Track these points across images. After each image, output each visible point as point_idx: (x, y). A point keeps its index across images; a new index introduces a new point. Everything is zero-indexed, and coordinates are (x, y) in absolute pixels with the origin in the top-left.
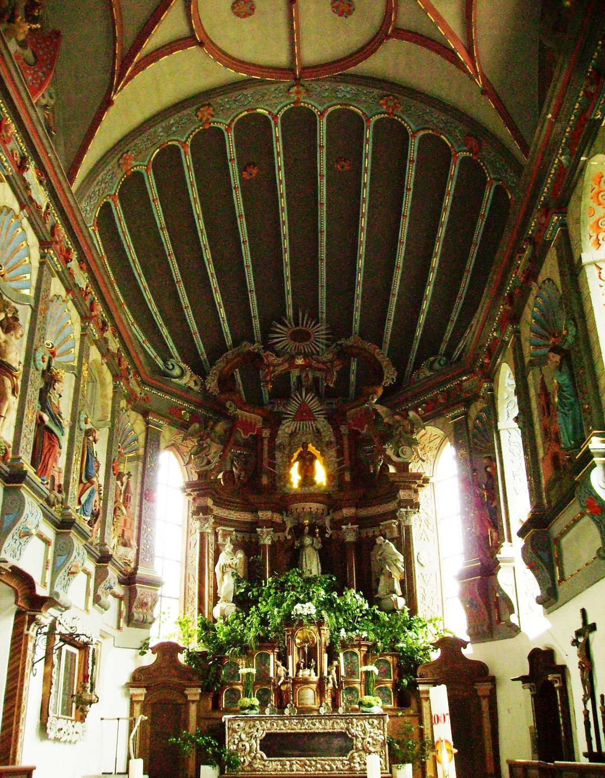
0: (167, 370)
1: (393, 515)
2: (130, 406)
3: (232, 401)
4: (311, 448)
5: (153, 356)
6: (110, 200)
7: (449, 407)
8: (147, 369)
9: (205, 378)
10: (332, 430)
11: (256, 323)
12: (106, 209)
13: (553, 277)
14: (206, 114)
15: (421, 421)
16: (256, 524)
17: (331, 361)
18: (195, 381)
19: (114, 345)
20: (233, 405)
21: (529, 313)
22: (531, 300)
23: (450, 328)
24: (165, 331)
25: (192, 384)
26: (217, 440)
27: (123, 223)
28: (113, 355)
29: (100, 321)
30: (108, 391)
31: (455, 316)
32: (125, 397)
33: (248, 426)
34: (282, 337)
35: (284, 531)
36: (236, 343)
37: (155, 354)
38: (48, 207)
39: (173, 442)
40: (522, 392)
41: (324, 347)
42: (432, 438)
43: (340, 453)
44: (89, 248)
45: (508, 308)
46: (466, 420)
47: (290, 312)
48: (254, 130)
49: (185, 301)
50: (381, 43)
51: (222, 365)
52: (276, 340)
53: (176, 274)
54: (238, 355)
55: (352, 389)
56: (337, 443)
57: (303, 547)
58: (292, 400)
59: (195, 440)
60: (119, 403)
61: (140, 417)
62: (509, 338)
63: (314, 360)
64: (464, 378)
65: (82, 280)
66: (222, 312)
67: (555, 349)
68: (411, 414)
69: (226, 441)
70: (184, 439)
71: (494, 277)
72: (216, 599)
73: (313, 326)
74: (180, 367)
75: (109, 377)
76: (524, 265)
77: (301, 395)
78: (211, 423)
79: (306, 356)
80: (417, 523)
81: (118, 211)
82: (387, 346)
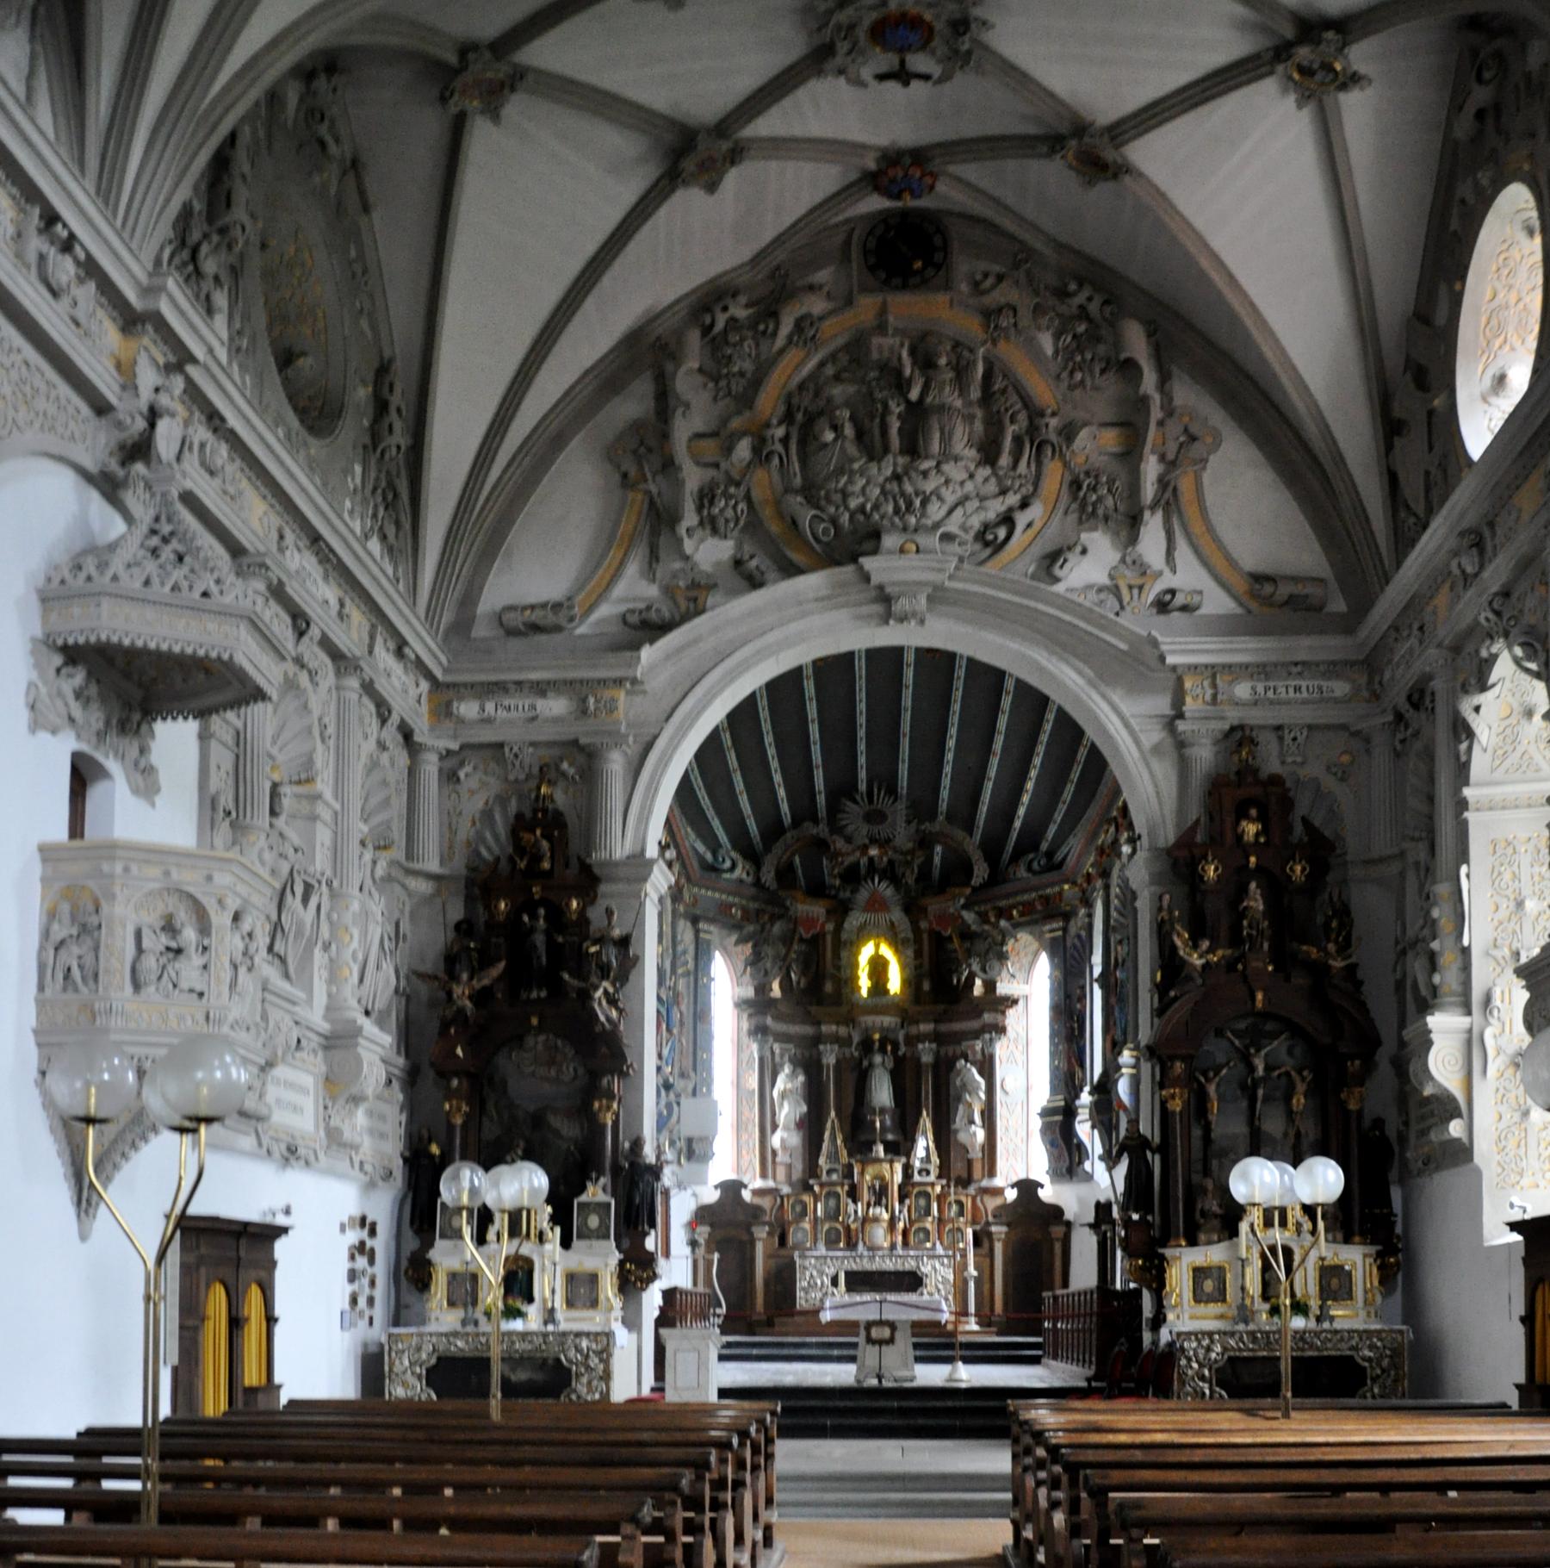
1: (976, 1035)
7: (1049, 917)
8: (696, 864)
11: (821, 800)
16: (817, 1040)
17: (912, 852)
23: (1052, 830)
31: (1058, 817)
33: (810, 922)
34: (853, 814)
35: (850, 1045)
36: (797, 822)
43: (918, 954)
46: (1064, 937)
47: (863, 787)
57: (871, 1065)
72: (775, 1127)
80: (1002, 1050)
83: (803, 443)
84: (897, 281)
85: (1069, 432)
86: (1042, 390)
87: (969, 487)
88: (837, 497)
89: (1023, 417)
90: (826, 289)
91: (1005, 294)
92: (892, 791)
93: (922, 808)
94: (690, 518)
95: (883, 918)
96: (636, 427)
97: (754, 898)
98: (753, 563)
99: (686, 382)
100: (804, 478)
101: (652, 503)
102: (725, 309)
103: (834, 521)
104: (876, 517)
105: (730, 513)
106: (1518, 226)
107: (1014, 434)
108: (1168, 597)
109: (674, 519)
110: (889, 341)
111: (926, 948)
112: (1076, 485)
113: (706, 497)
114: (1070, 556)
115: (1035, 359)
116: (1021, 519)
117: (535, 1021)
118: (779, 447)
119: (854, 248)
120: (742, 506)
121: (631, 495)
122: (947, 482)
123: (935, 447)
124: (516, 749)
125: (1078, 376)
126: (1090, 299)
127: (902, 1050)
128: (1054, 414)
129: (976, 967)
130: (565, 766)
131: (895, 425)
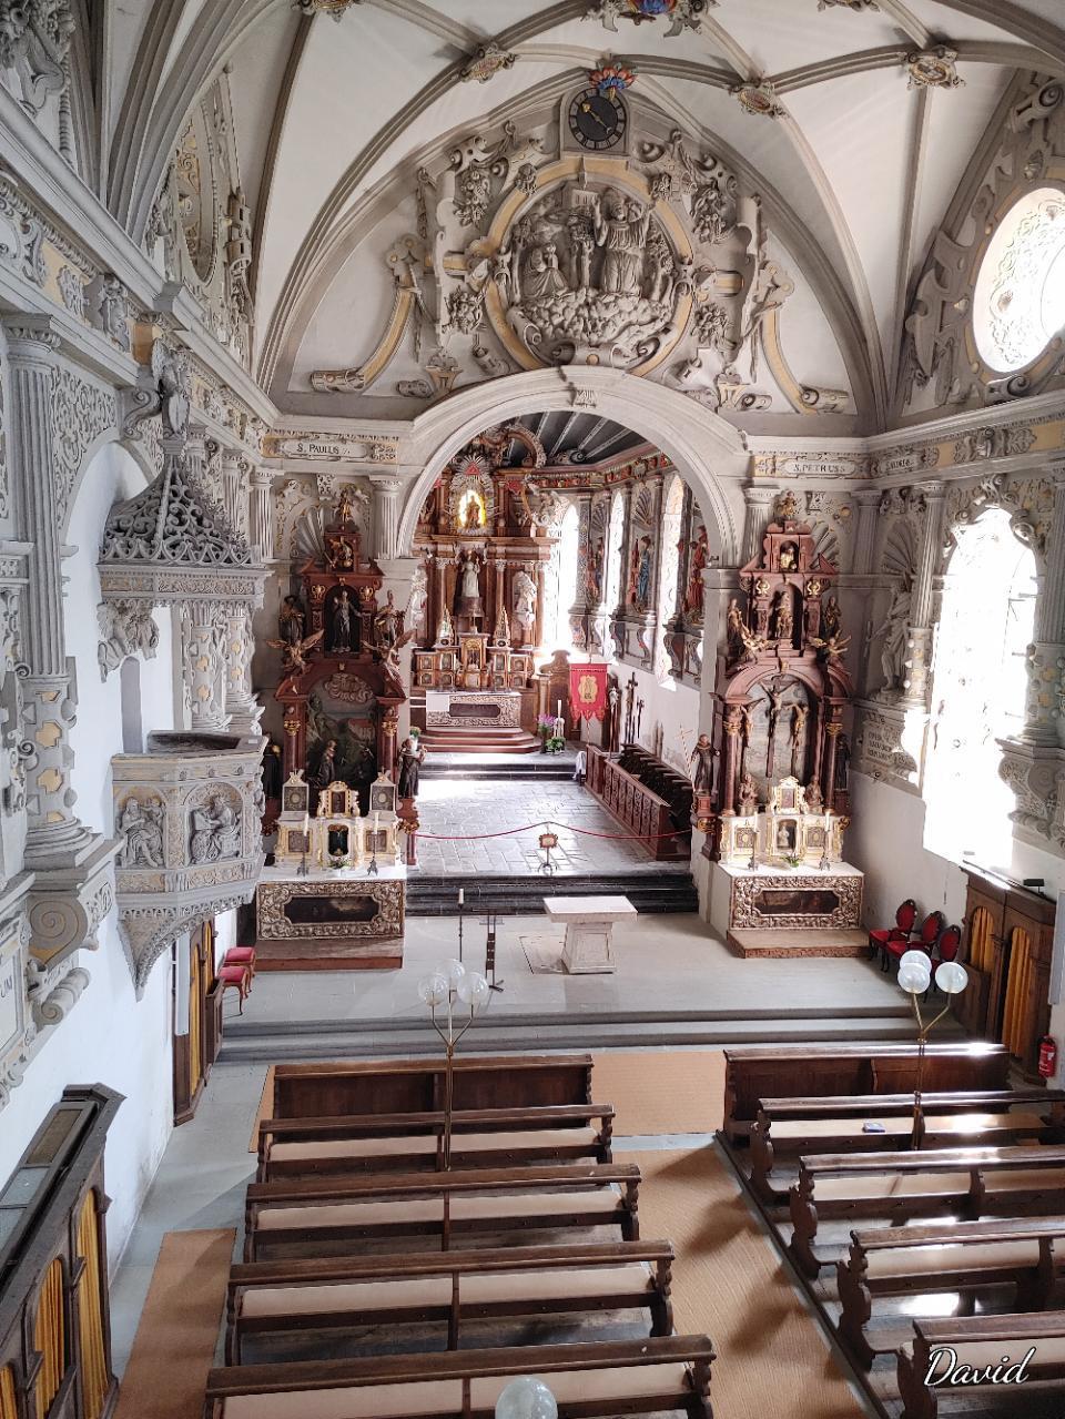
7: (580, 491)
43: (497, 503)
83: (522, 266)
84: (590, 144)
85: (700, 275)
86: (684, 240)
87: (633, 318)
88: (545, 315)
89: (669, 262)
90: (542, 144)
91: (663, 164)
94: (444, 317)
96: (405, 239)
98: (487, 358)
99: (445, 213)
100: (522, 294)
101: (417, 301)
102: (471, 152)
103: (542, 331)
104: (571, 331)
105: (470, 316)
106: (1044, 207)
107: (666, 273)
108: (750, 400)
109: (435, 320)
110: (584, 193)
112: (700, 315)
113: (456, 302)
114: (691, 368)
115: (675, 215)
116: (664, 339)
117: (342, 667)
118: (506, 271)
119: (562, 108)
120: (479, 311)
121: (402, 293)
122: (620, 312)
123: (614, 286)
124: (325, 480)
125: (707, 232)
126: (720, 175)
127: (485, 561)
128: (690, 263)
130: (358, 493)
131: (587, 262)
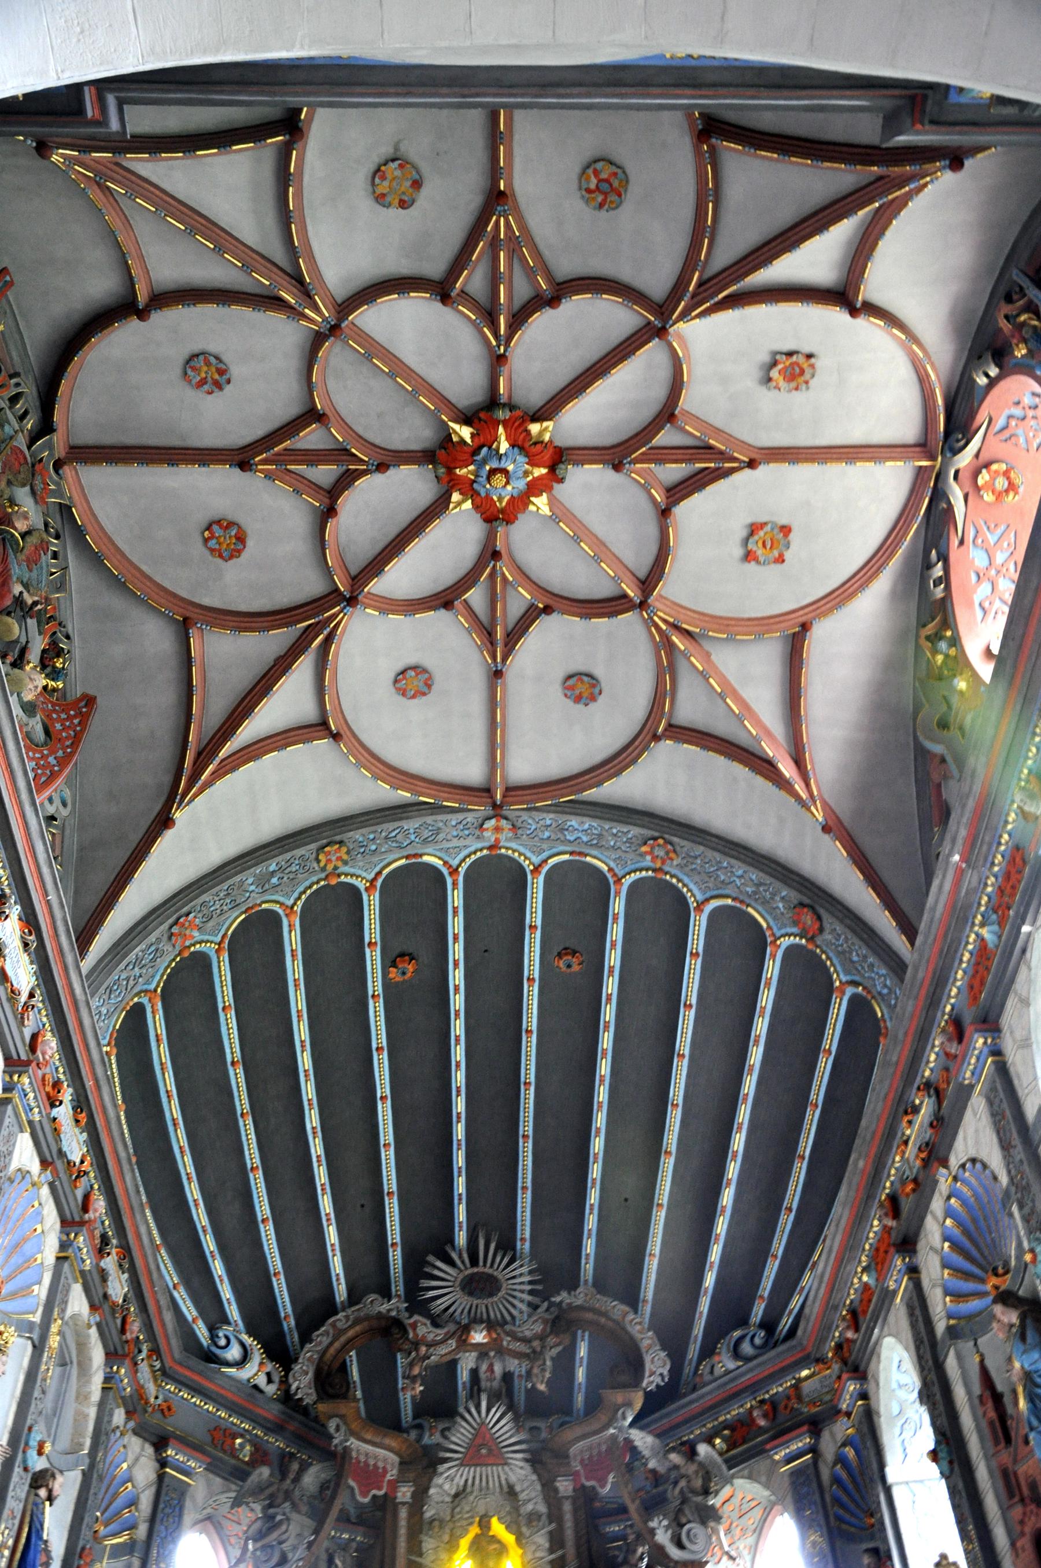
0: (214, 1349)
2: (131, 1424)
3: (342, 1417)
4: (498, 1528)
5: (190, 1319)
6: (145, 1000)
7: (781, 1433)
8: (174, 1342)
9: (287, 1369)
10: (539, 1487)
11: (396, 1257)
12: (136, 1016)
13: (983, 1155)
14: (334, 858)
15: (724, 1467)
17: (542, 1338)
18: (268, 1374)
19: (118, 1288)
20: (343, 1428)
21: (935, 1232)
22: (937, 1205)
23: (772, 1268)
24: (218, 1268)
25: (261, 1380)
26: (304, 1509)
27: (164, 1048)
28: (114, 1306)
29: (97, 1233)
30: (93, 1388)
32: (124, 1401)
33: (370, 1476)
34: (446, 1290)
36: (354, 1297)
37: (195, 1313)
38: (31, 995)
39: (209, 1510)
40: (936, 1393)
41: (524, 1307)
42: (745, 1507)
43: (556, 1541)
44: (96, 1081)
45: (890, 1223)
47: (461, 1238)
48: (416, 892)
49: (263, 1208)
50: (646, 748)
51: (326, 1341)
52: (432, 1294)
53: (252, 1154)
54: (357, 1322)
55: (580, 1399)
56: (551, 1517)
58: (459, 1419)
59: (258, 1507)
60: (111, 1415)
61: (149, 1450)
62: (898, 1283)
63: (508, 1334)
64: (805, 1373)
65: (75, 1145)
66: (332, 1235)
67: (1006, 1298)
68: (703, 1449)
69: (320, 1506)
70: (237, 1503)
71: (859, 1163)
73: (504, 1269)
74: (242, 1344)
75: (97, 1355)
76: (918, 1136)
77: (479, 1412)
78: (295, 1466)
79: (491, 1325)
81: (157, 1023)
82: (648, 1309)
92: (507, 1245)
93: (556, 1273)
95: (494, 1475)
97: (276, 1428)
111: (569, 1533)
129: (663, 1537)
